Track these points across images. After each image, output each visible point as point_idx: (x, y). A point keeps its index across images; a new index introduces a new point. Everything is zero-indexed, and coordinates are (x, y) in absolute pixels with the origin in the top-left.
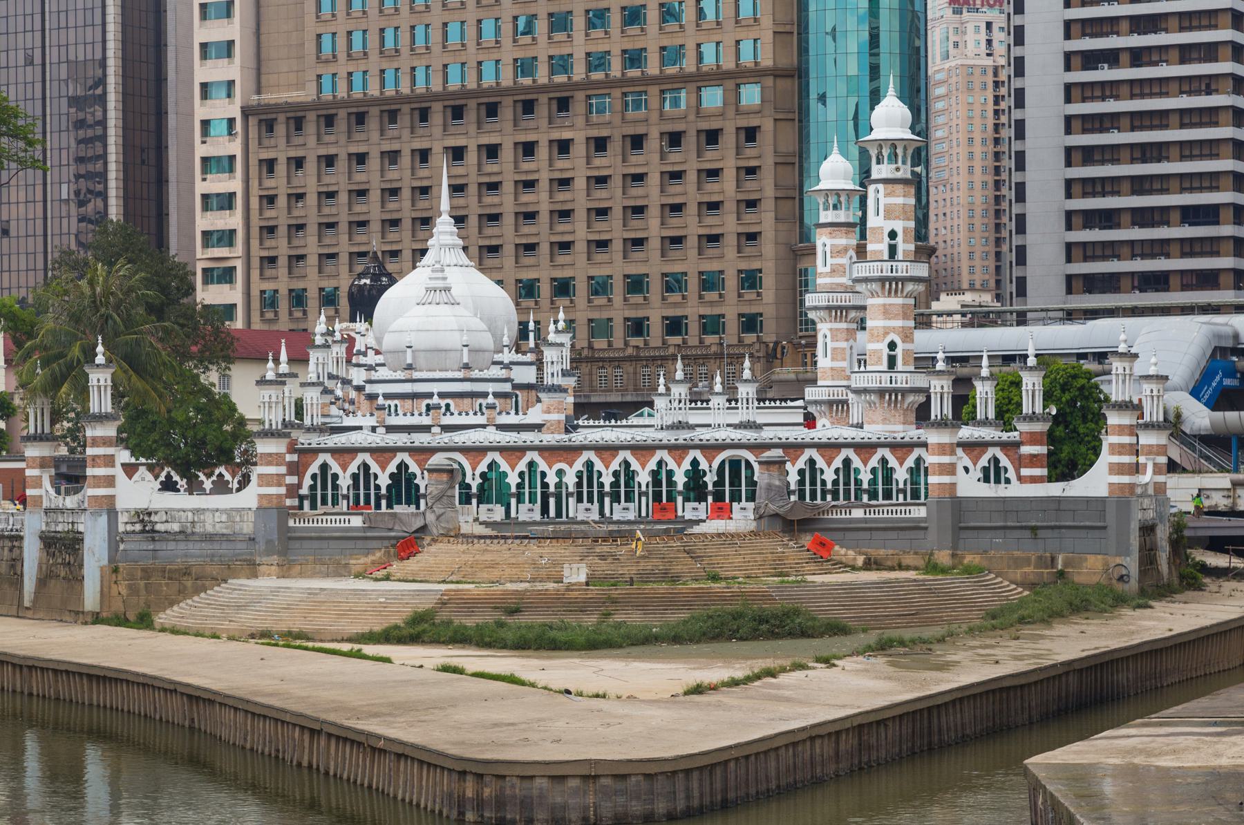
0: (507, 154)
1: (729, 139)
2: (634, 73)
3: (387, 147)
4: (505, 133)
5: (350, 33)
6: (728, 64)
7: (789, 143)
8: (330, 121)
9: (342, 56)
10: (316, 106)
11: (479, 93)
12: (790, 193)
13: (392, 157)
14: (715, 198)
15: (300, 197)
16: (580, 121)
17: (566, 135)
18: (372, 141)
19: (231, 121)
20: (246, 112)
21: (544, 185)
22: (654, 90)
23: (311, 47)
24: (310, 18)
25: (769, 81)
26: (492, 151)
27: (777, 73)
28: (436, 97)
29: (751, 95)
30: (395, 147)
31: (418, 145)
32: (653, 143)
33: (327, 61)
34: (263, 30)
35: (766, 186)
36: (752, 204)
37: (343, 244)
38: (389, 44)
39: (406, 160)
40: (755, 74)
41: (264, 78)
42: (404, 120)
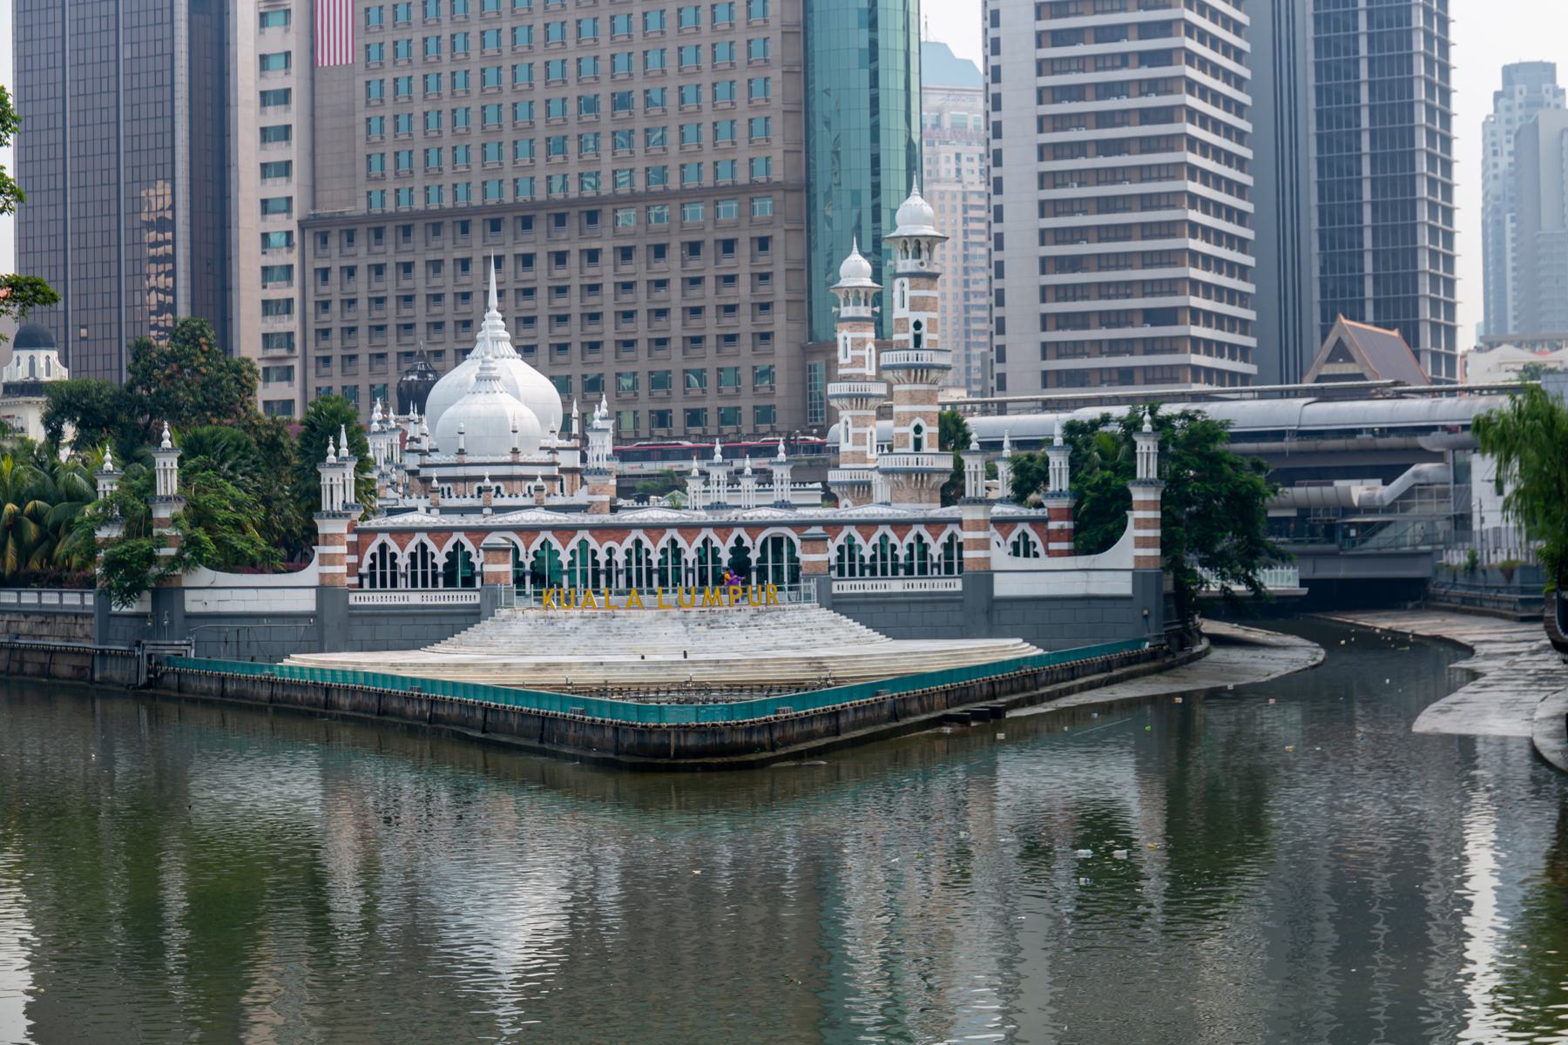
0: (541, 263)
1: (744, 249)
3: (432, 256)
4: (539, 243)
5: (397, 154)
6: (742, 178)
7: (797, 252)
8: (379, 233)
9: (390, 173)
10: (368, 218)
11: (515, 206)
12: (800, 297)
13: (436, 266)
14: (732, 302)
15: (352, 302)
16: (608, 232)
17: (595, 245)
18: (419, 251)
19: (289, 234)
20: (302, 226)
21: (575, 291)
23: (361, 167)
25: (779, 195)
26: (528, 260)
28: (477, 211)
29: (764, 207)
30: (439, 256)
31: (459, 254)
32: (675, 252)
33: (376, 179)
34: (318, 151)
35: (779, 290)
36: (765, 307)
37: (392, 346)
38: (433, 162)
39: (448, 268)
40: (769, 188)
41: (318, 195)
42: (447, 232)
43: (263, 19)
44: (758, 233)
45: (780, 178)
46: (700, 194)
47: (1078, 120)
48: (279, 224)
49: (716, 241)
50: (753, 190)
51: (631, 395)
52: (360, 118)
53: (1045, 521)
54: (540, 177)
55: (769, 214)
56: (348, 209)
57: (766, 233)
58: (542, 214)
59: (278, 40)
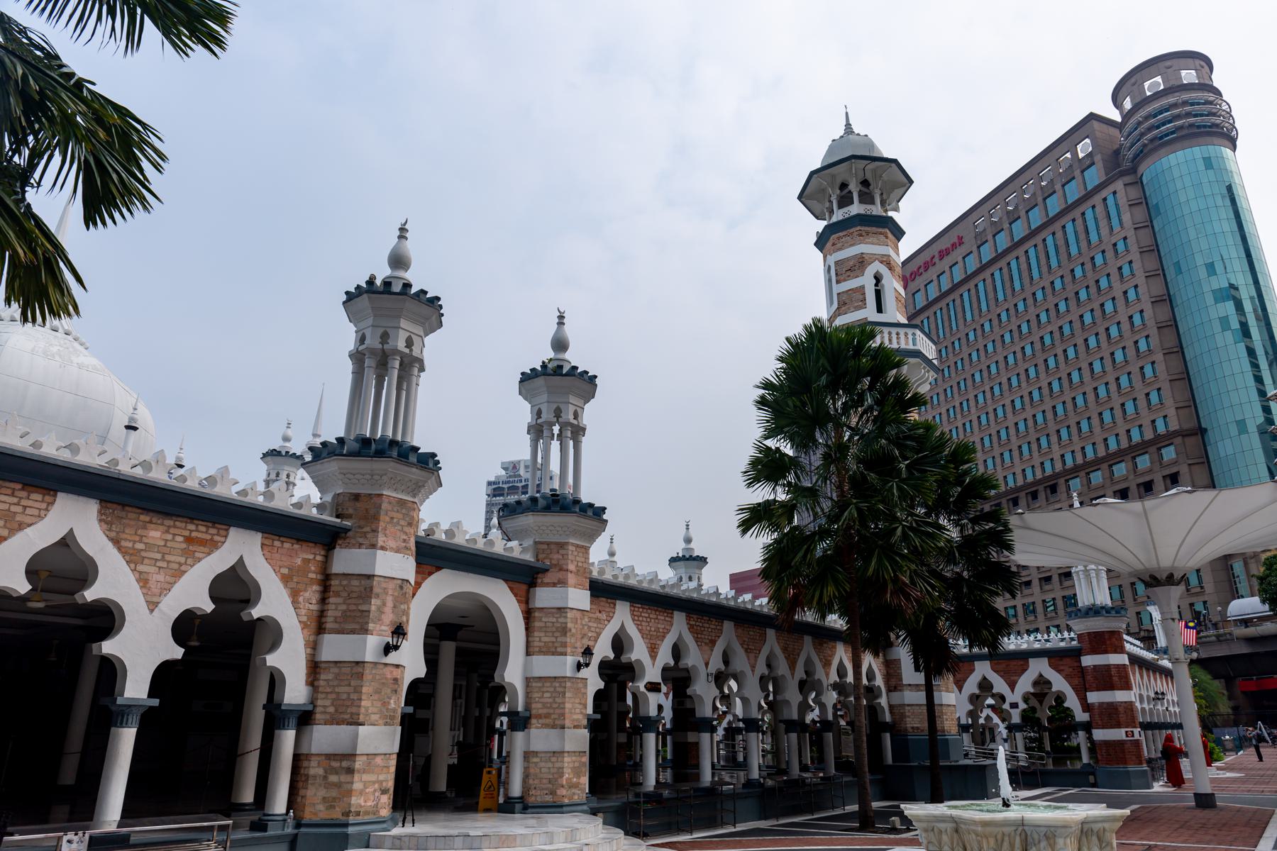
25: (1178, 440)
27: (1183, 434)
29: (1169, 453)
44: (1167, 472)
45: (1177, 427)
46: (1118, 456)
49: (1138, 485)
50: (1159, 442)
51: (1199, 590)
53: (1075, 654)
54: (1057, 457)
55: (1174, 456)
57: (1174, 470)
58: (1022, 494)
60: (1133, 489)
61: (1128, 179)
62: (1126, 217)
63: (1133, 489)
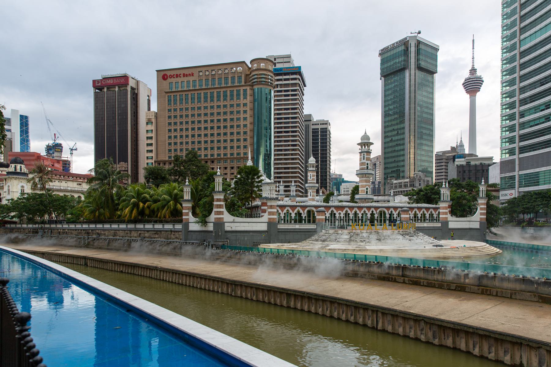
2: (225, 157)
20: (155, 162)
22: (229, 161)
23: (167, 151)
24: (167, 147)
32: (229, 169)
43: (147, 123)
47: (281, 155)
48: (150, 161)
52: (167, 142)
56: (164, 159)
59: (150, 127)
60: (235, 167)
61: (251, 87)
62: (248, 97)
63: (235, 167)
